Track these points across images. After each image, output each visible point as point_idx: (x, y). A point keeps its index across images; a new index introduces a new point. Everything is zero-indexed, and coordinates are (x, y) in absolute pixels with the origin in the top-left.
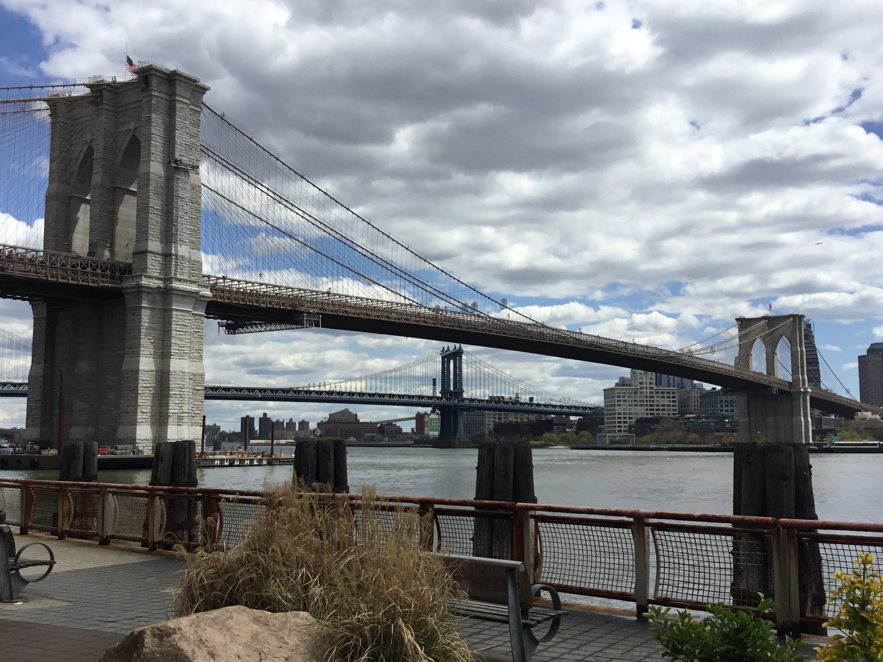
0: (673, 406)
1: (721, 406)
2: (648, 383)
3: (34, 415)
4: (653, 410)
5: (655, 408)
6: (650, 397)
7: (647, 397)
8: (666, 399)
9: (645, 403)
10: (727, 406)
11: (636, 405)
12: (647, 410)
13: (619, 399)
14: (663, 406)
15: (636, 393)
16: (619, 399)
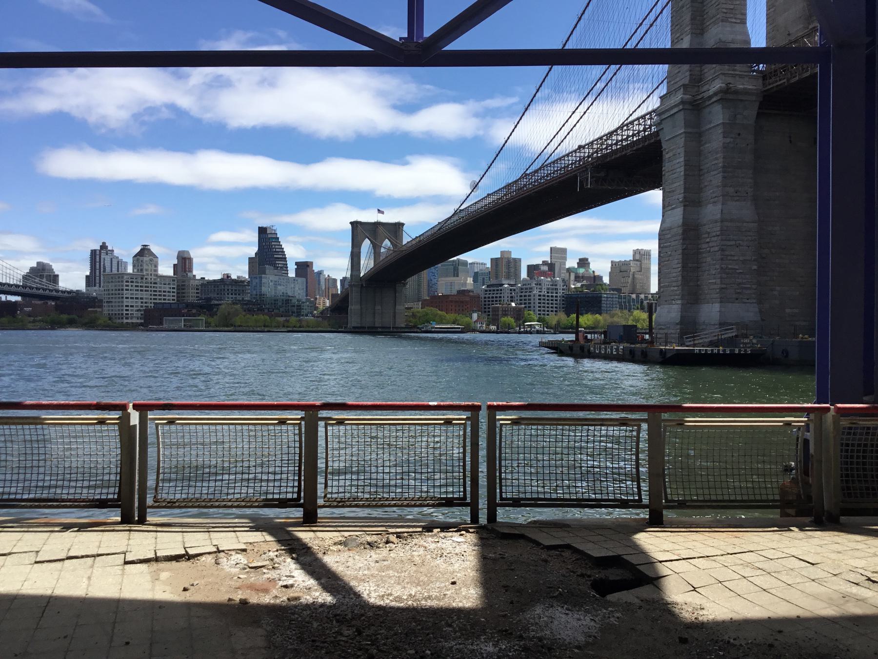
0: (173, 292)
1: (228, 294)
2: (153, 271)
3: (740, 284)
4: (156, 295)
5: (158, 293)
6: (155, 283)
7: (151, 283)
8: (167, 286)
9: (149, 289)
10: (232, 294)
11: (142, 291)
12: (151, 295)
13: (127, 284)
14: (164, 292)
15: (142, 279)
16: (127, 284)
